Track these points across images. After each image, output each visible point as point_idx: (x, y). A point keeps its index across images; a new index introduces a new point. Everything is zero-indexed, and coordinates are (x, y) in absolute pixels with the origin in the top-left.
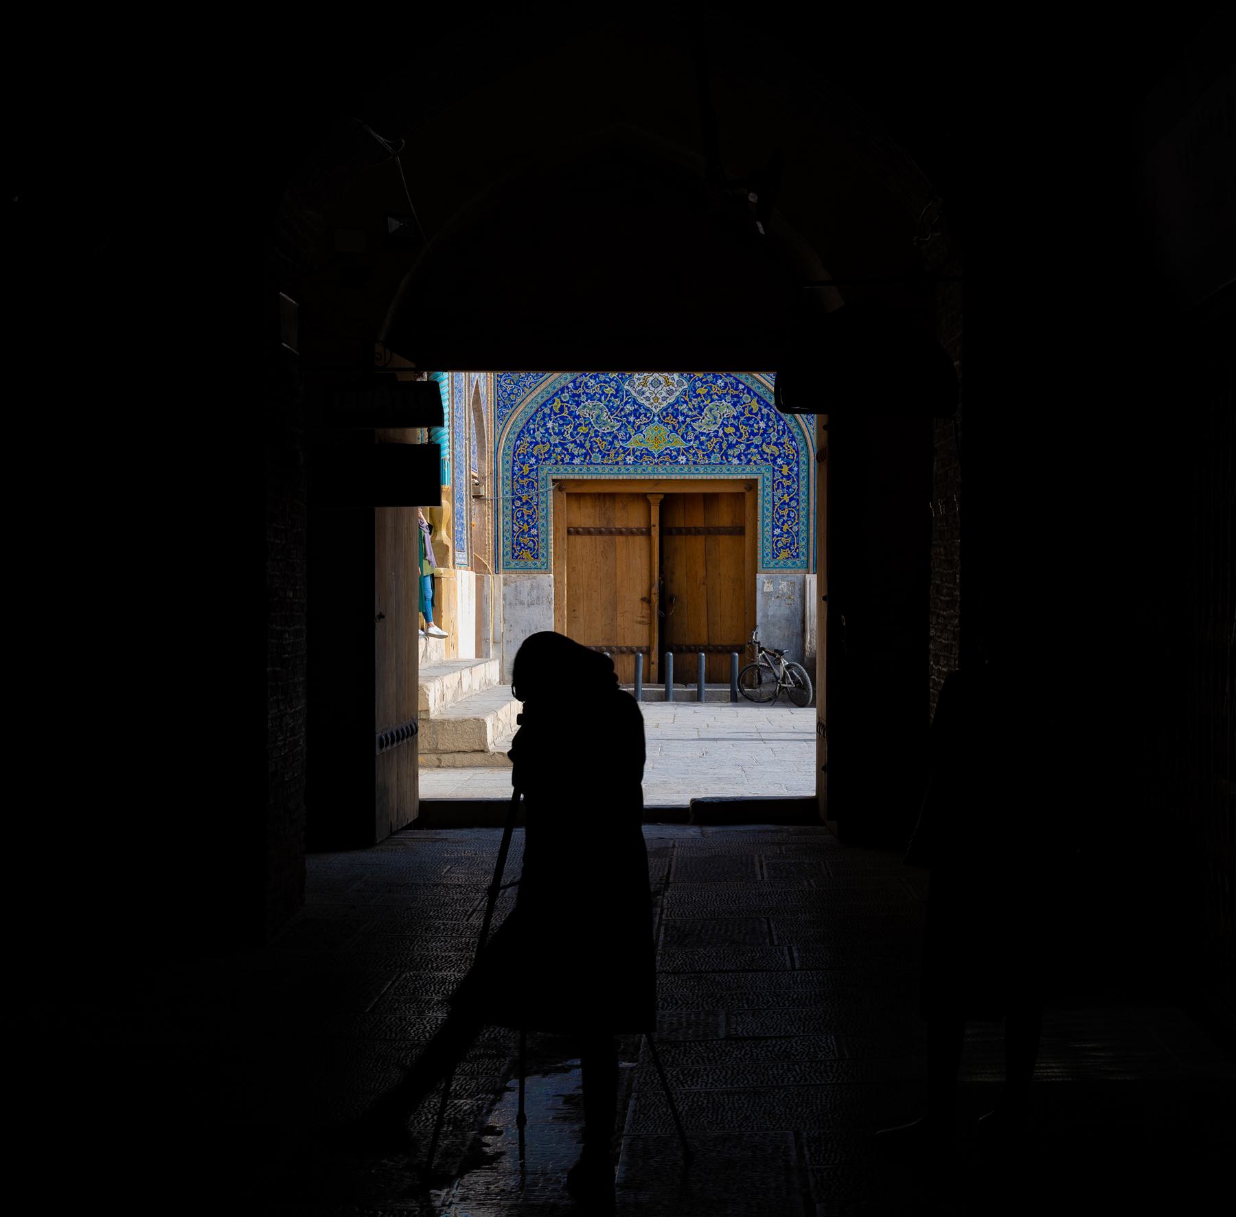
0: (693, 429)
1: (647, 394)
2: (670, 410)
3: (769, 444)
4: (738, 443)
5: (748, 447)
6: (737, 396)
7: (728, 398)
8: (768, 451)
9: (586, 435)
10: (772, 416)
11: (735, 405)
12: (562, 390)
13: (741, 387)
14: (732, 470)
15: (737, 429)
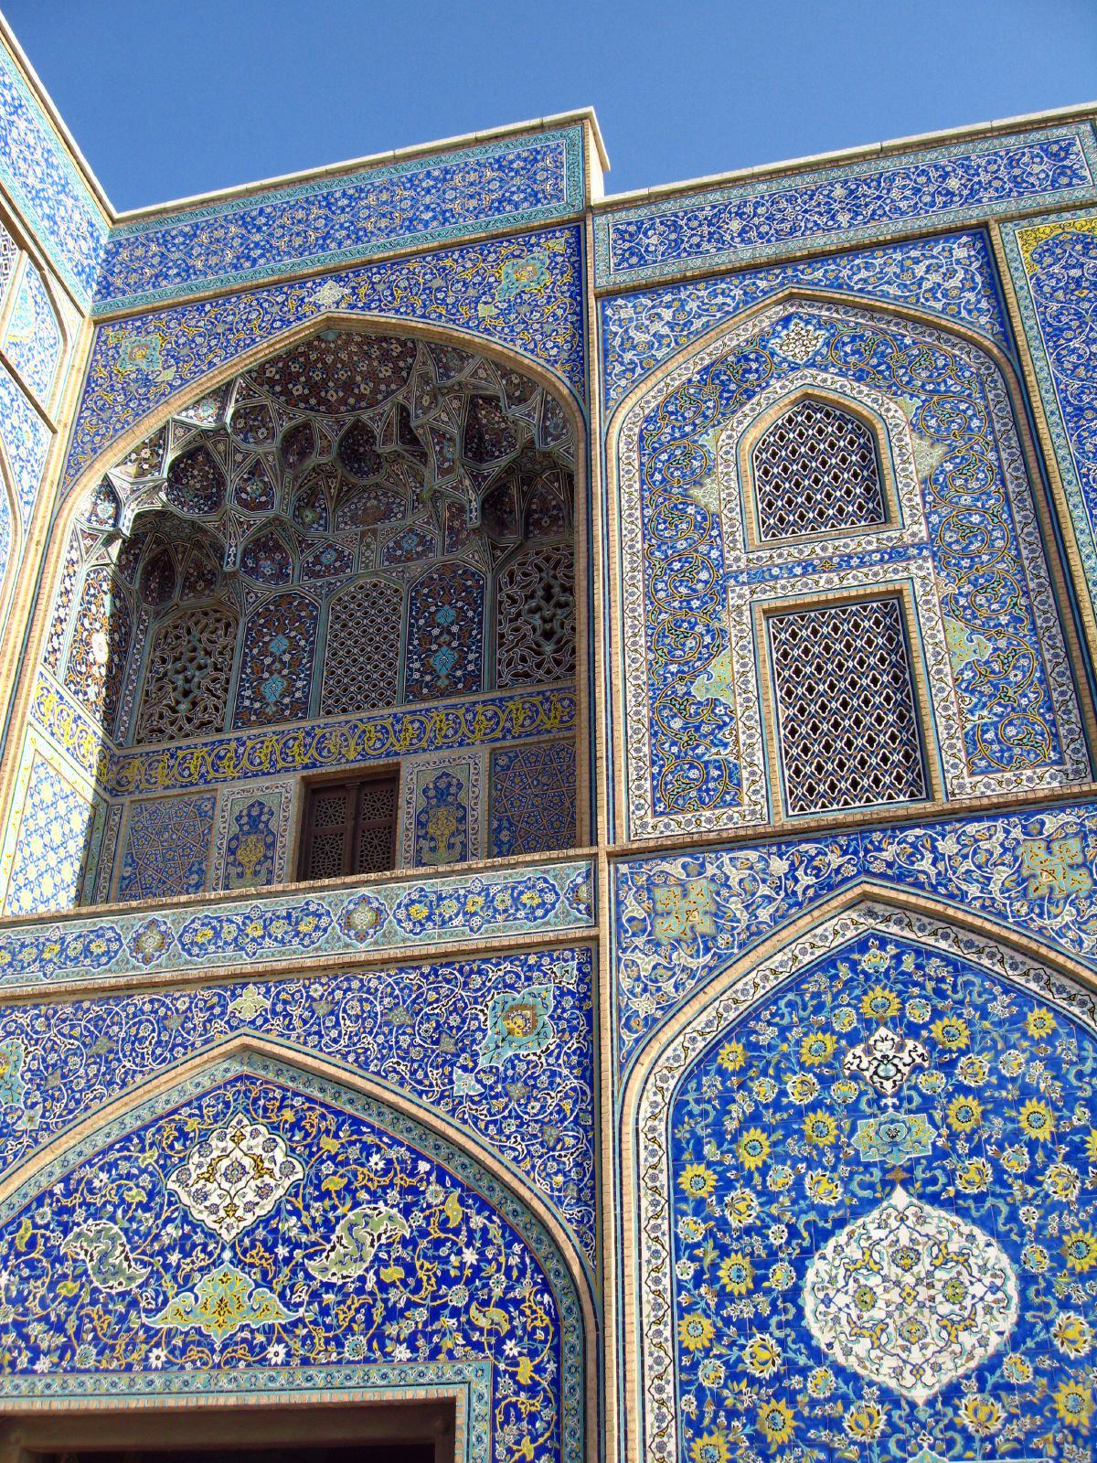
0: (309, 1277)
1: (214, 1199)
2: (261, 1233)
3: (485, 1303)
4: (410, 1305)
5: (435, 1314)
6: (413, 1190)
7: (393, 1195)
8: (483, 1322)
9: (72, 1301)
10: (494, 1231)
11: (406, 1211)
12: (40, 1201)
13: (423, 1167)
14: (393, 1376)
15: (410, 1270)
